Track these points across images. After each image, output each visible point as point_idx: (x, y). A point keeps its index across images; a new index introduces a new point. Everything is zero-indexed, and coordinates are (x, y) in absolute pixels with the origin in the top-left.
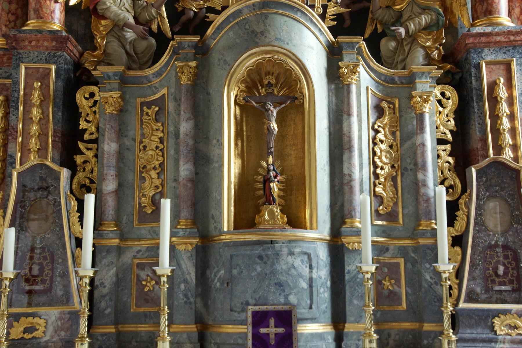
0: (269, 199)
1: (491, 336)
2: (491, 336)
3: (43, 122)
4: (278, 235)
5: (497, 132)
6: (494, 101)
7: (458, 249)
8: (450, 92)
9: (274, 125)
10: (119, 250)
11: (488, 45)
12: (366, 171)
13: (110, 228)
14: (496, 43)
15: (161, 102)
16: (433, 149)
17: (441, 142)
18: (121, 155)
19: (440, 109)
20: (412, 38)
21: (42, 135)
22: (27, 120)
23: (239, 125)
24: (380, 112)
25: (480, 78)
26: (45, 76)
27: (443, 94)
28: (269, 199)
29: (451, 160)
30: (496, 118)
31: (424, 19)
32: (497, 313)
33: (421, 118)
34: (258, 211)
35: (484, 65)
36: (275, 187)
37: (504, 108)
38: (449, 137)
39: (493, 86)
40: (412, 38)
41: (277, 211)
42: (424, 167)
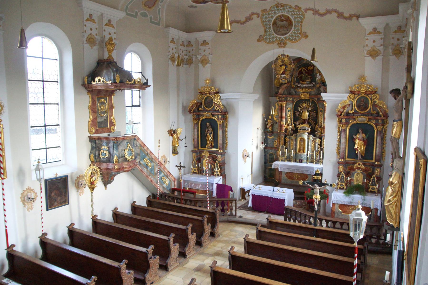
0: (301, 150)
3: (283, 141)
4: (301, 153)
6: (323, 141)
8: (320, 140)
9: (302, 143)
10: (289, 153)
12: (311, 147)
13: (288, 151)
15: (293, 140)
18: (289, 144)
20: (318, 133)
21: (283, 142)
22: (281, 141)
23: (299, 143)
24: (313, 142)
26: (283, 137)
28: (301, 150)
31: (319, 131)
33: (316, 143)
34: (300, 151)
36: (302, 149)
40: (318, 133)
41: (302, 151)
42: (316, 147)
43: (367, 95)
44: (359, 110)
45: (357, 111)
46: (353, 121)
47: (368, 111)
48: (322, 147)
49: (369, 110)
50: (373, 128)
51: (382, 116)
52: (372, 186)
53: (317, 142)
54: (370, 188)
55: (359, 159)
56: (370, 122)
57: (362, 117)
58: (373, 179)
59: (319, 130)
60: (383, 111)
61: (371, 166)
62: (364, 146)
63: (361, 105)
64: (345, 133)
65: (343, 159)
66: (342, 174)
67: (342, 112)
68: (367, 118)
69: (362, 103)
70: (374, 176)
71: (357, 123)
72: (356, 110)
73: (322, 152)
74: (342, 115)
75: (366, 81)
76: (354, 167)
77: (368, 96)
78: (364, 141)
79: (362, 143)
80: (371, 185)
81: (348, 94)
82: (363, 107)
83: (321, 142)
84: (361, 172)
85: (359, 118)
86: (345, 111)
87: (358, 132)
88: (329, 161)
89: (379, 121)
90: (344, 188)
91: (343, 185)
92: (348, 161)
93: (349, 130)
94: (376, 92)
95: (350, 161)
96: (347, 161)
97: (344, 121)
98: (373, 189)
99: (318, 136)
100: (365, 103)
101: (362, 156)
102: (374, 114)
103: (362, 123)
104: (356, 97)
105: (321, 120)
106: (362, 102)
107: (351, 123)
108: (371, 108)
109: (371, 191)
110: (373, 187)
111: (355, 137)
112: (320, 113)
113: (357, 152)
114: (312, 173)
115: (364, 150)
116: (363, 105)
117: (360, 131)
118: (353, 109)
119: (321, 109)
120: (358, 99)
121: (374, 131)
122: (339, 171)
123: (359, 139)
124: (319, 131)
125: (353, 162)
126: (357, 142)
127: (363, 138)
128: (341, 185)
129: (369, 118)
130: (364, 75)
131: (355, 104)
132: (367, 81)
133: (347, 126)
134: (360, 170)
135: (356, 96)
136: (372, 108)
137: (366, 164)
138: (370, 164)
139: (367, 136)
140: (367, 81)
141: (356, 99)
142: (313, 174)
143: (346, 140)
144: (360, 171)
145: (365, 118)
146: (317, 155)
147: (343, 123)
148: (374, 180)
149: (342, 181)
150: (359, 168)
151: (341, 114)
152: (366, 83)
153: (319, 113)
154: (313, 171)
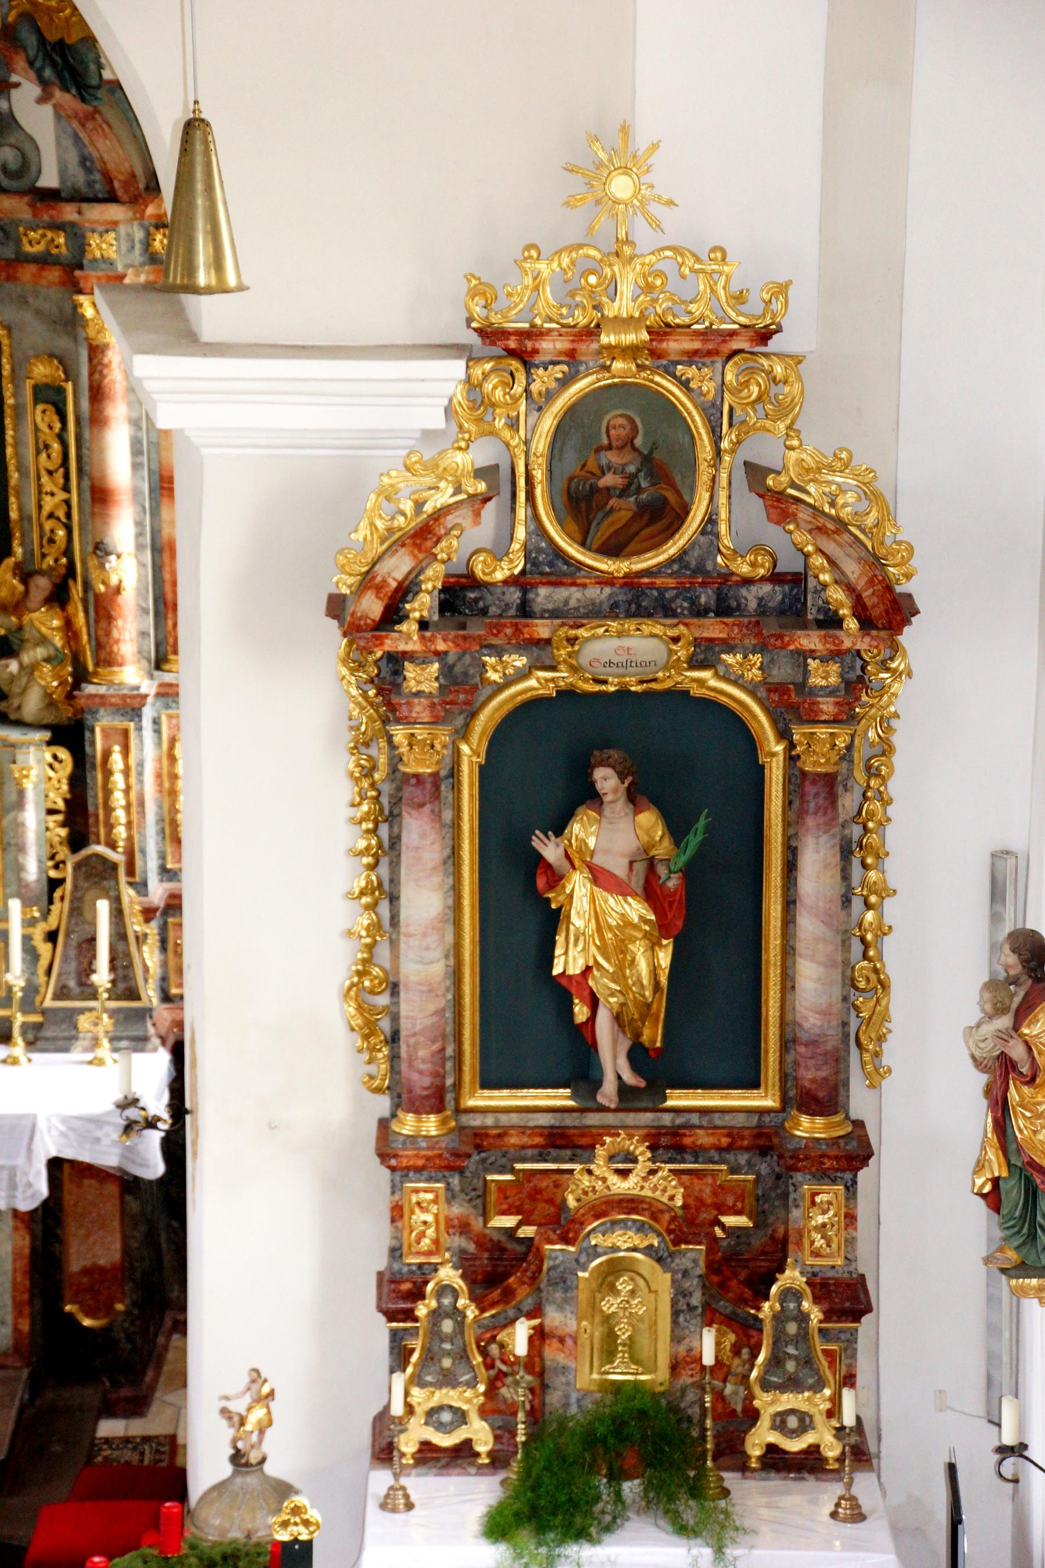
1: (73, 1033)
2: (73, 1033)
5: (109, 810)
6: (108, 773)
7: (49, 945)
8: (64, 754)
11: (103, 704)
14: (111, 705)
16: (39, 823)
17: (51, 812)
19: (51, 773)
25: (93, 743)
27: (55, 757)
29: (63, 832)
30: (108, 792)
31: (40, 652)
32: (82, 1011)
33: (21, 793)
35: (98, 730)
37: (118, 779)
38: (61, 805)
39: (107, 754)
40: (29, 670)
42: (21, 849)
43: (669, 372)
44: (583, 544)
45: (566, 559)
46: (523, 675)
47: (684, 552)
48: (100, 849)
49: (692, 544)
50: (750, 744)
51: (852, 624)
52: (783, 1388)
53: (28, 785)
54: (765, 1421)
55: (609, 1088)
56: (706, 675)
57: (620, 635)
58: (779, 1318)
59: (44, 641)
60: (853, 570)
61: (743, 1158)
62: (654, 946)
63: (608, 480)
64: (437, 815)
65: (438, 1108)
66: (443, 1290)
67: (406, 590)
68: (676, 640)
69: (612, 457)
70: (792, 1277)
71: (567, 695)
72: (551, 541)
73: (103, 907)
74: (410, 627)
75: (655, 209)
76: (571, 1202)
77: (685, 384)
78: (651, 893)
79: (636, 909)
80: (766, 1386)
81: (457, 368)
82: (624, 509)
83: (78, 781)
84: (649, 1250)
85: (594, 637)
86: (433, 578)
87: (591, 796)
88: (273, 1127)
89: (812, 664)
90: (467, 1443)
91: (461, 1417)
92: (489, 1120)
93: (486, 773)
94: (764, 336)
95: (514, 1119)
96: (476, 1121)
97: (430, 686)
98: (793, 1422)
99: (32, 705)
100: (647, 460)
101: (638, 1055)
102: (747, 581)
103: (623, 693)
104: (549, 396)
105: (49, 503)
106: (610, 447)
107: (500, 688)
108: (711, 520)
109: (772, 1448)
110: (788, 1401)
111: (551, 851)
112: (42, 417)
113: (581, 1012)
114: (13, 1186)
115: (657, 987)
116: (624, 492)
117: (606, 780)
118: (521, 533)
119: (42, 371)
120: (571, 413)
121: (761, 769)
122: (396, 1252)
123: (599, 877)
124: (40, 652)
125: (544, 1120)
126: (579, 917)
127: (640, 868)
128: (432, 1413)
129: (697, 642)
130: (625, 130)
131: (539, 475)
132: (671, 203)
133: (464, 733)
134: (641, 1228)
135: (543, 379)
136: (723, 514)
137: (687, 1141)
138: (732, 1133)
139: (694, 840)
140: (671, 203)
141: (548, 423)
142: (25, 1205)
143: (456, 890)
144: (637, 1240)
145: (655, 642)
146: (45, 949)
147: (420, 710)
148: (792, 1328)
149: (447, 1363)
150: (630, 1204)
151: (393, 615)
152: (656, 225)
153: (18, 410)
154: (20, 1161)
